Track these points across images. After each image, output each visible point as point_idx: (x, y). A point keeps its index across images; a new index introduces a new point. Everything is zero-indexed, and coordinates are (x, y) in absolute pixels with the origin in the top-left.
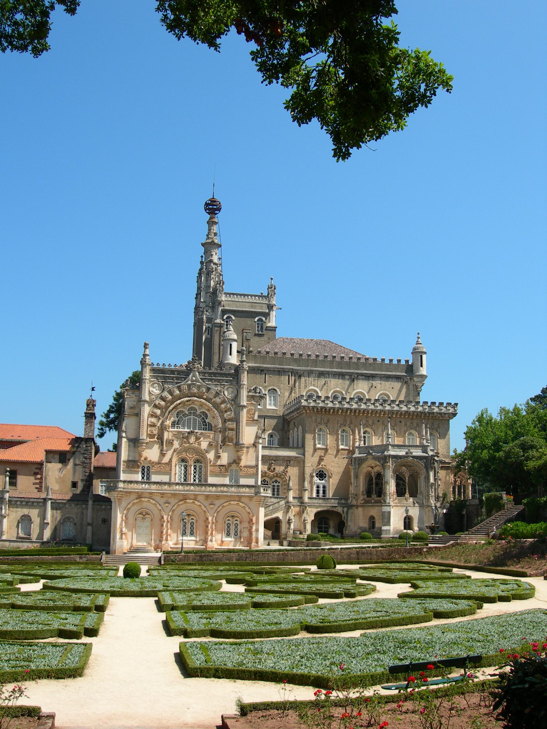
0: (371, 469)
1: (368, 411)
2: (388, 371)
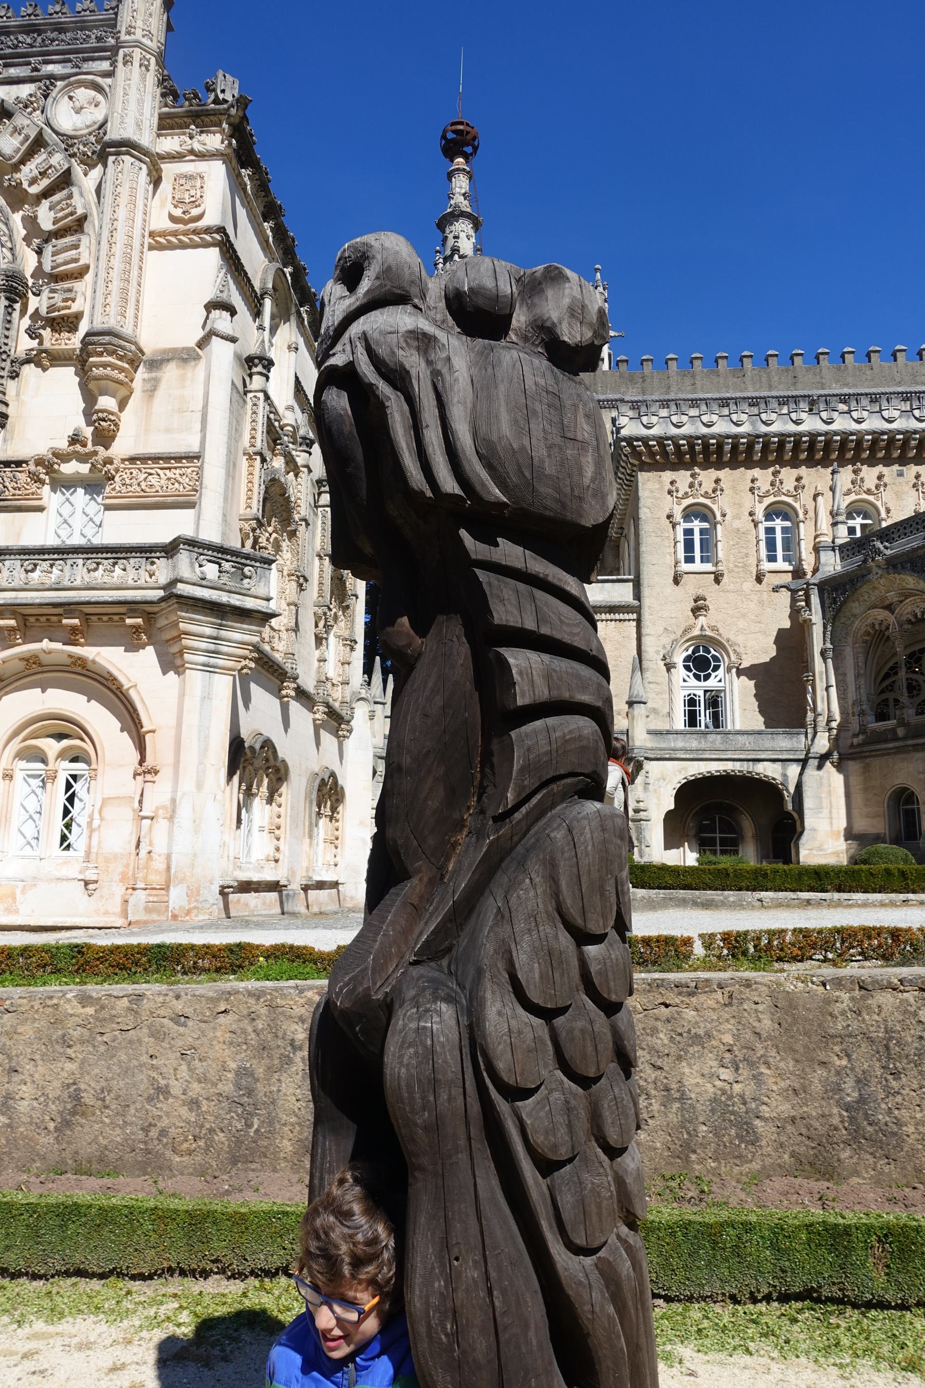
0: (881, 614)
1: (859, 442)
2: (917, 383)
